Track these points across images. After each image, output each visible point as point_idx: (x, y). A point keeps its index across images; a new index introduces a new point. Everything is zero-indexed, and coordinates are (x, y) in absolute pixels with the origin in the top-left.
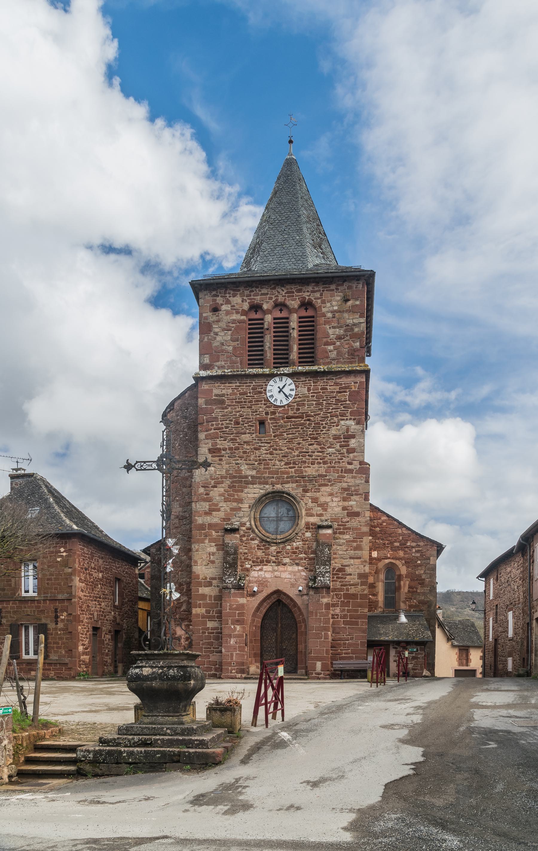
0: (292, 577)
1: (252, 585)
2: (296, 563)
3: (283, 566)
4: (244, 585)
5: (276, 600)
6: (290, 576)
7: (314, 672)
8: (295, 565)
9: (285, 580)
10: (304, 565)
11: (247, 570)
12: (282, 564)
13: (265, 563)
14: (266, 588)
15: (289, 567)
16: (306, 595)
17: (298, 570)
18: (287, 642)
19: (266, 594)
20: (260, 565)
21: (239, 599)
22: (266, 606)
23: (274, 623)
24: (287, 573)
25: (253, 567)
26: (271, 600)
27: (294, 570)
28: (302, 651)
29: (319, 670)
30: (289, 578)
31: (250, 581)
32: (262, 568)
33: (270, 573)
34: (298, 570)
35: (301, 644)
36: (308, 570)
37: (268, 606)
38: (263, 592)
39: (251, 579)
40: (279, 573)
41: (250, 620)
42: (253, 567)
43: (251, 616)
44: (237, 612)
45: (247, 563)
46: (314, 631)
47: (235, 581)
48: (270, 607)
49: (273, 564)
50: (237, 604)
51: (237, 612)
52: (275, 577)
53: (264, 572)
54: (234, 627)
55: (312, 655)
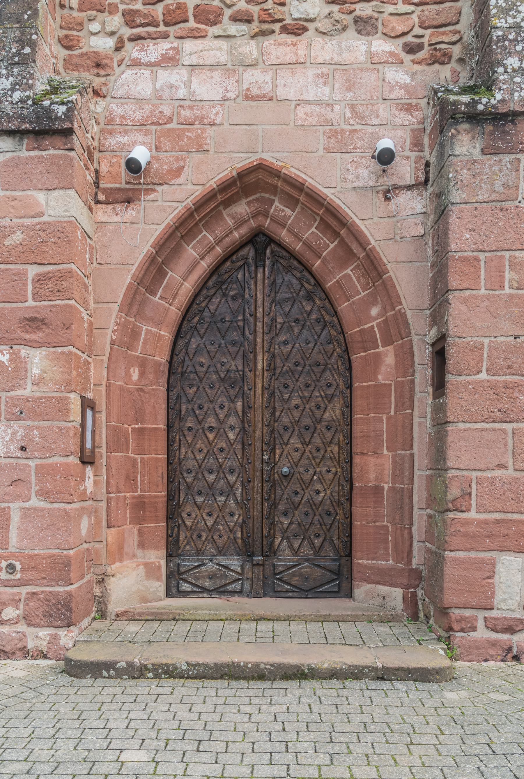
0: (338, 97)
1: (124, 140)
2: (357, 20)
3: (290, 39)
4: (70, 111)
5: (244, 230)
6: (324, 92)
7: (481, 615)
8: (351, 32)
9: (301, 112)
10: (401, 28)
11: (98, 65)
12: (285, 29)
13: (192, 23)
14: (196, 157)
15: (319, 41)
16: (409, 188)
17: (371, 55)
18: (295, 442)
19: (199, 192)
20: (166, 36)
21: (41, 197)
22: (195, 265)
23: (233, 349)
24: (311, 73)
25: (129, 45)
26: (219, 232)
27: (346, 57)
28: (378, 490)
29: (513, 604)
30: (319, 103)
31: (110, 121)
32: (176, 50)
33: (217, 75)
34: (371, 55)
35: (376, 453)
36: (421, 55)
37: (205, 265)
38: (182, 180)
39: (117, 109)
40: (268, 78)
41: (112, 326)
42: (129, 45)
43: (116, 307)
44: (33, 271)
45: (95, 27)
46: (483, 376)
47: (17, 95)
48: (215, 270)
49: (233, 29)
50: (32, 228)
51: (33, 271)
52: (248, 97)
53: (184, 72)
54: (15, 358)
55: (473, 514)
